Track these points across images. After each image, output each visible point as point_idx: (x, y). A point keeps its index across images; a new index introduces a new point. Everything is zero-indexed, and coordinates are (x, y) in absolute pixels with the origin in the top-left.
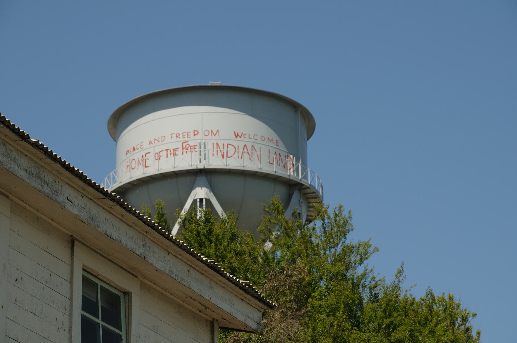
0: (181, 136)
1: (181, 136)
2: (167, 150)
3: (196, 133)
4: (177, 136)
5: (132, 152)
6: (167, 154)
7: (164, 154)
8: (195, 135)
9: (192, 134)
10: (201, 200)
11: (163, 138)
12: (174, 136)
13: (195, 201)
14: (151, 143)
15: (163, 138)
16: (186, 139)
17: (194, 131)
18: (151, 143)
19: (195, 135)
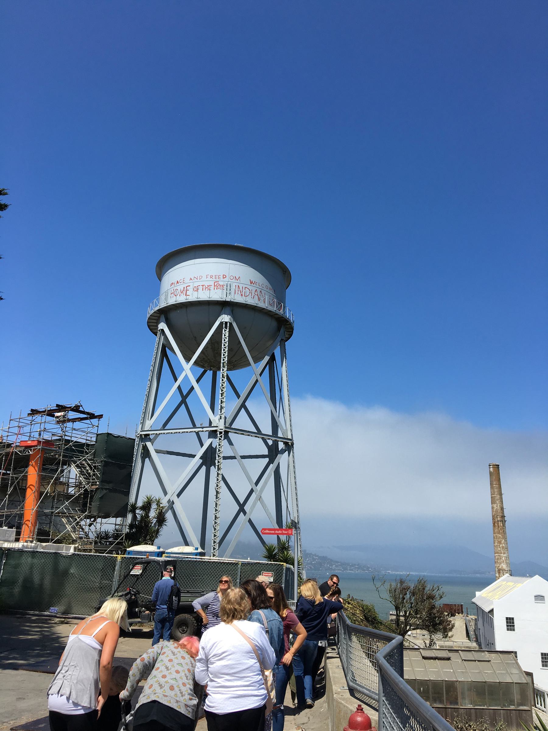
0: (214, 277)
1: (214, 277)
2: (203, 286)
3: (224, 276)
4: (211, 277)
5: (176, 284)
6: (203, 288)
7: (201, 288)
8: (223, 278)
9: (222, 277)
10: (226, 323)
11: (201, 277)
12: (209, 276)
13: (221, 323)
14: (191, 279)
15: (201, 277)
16: (218, 280)
17: (223, 275)
18: (191, 279)
19: (223, 278)
